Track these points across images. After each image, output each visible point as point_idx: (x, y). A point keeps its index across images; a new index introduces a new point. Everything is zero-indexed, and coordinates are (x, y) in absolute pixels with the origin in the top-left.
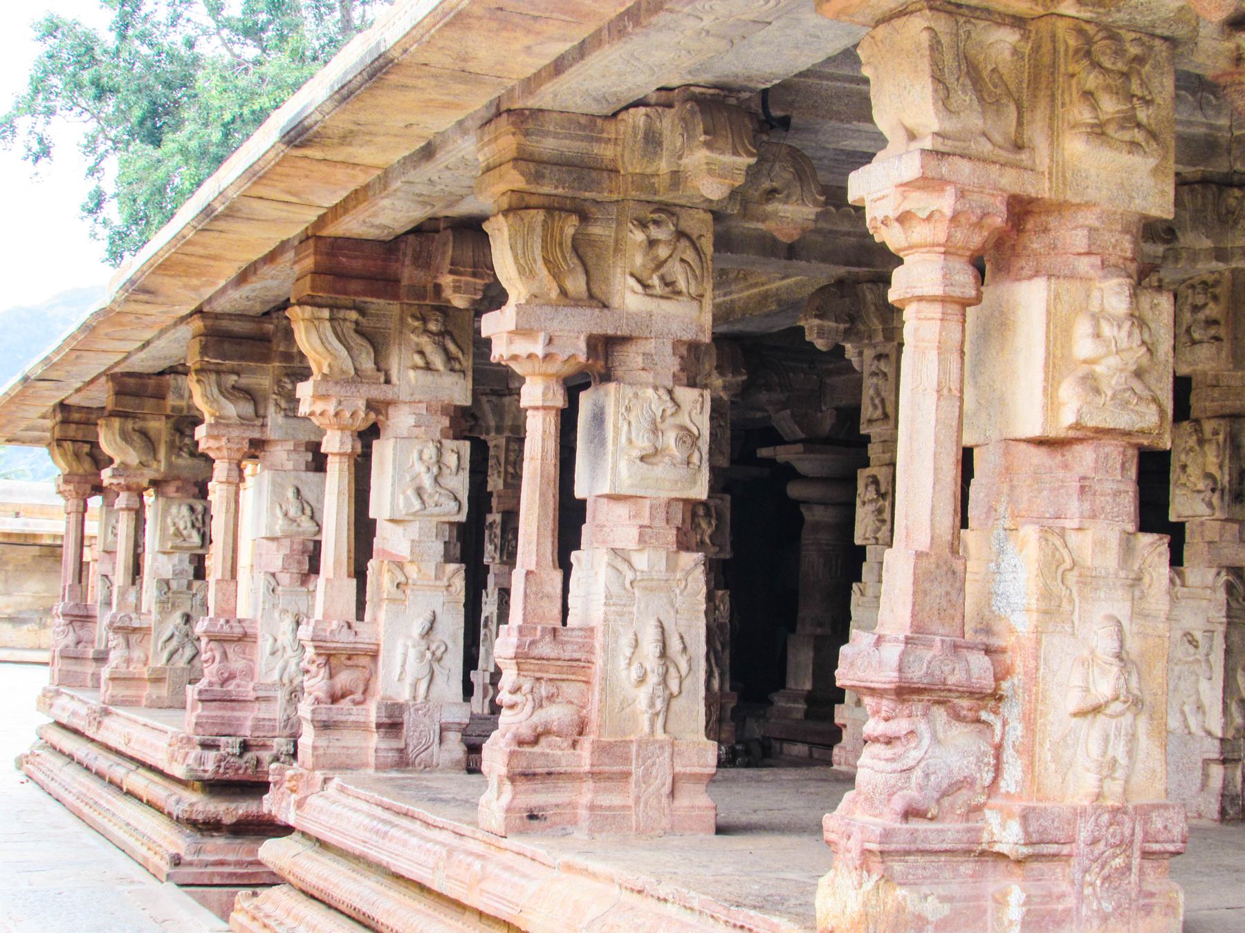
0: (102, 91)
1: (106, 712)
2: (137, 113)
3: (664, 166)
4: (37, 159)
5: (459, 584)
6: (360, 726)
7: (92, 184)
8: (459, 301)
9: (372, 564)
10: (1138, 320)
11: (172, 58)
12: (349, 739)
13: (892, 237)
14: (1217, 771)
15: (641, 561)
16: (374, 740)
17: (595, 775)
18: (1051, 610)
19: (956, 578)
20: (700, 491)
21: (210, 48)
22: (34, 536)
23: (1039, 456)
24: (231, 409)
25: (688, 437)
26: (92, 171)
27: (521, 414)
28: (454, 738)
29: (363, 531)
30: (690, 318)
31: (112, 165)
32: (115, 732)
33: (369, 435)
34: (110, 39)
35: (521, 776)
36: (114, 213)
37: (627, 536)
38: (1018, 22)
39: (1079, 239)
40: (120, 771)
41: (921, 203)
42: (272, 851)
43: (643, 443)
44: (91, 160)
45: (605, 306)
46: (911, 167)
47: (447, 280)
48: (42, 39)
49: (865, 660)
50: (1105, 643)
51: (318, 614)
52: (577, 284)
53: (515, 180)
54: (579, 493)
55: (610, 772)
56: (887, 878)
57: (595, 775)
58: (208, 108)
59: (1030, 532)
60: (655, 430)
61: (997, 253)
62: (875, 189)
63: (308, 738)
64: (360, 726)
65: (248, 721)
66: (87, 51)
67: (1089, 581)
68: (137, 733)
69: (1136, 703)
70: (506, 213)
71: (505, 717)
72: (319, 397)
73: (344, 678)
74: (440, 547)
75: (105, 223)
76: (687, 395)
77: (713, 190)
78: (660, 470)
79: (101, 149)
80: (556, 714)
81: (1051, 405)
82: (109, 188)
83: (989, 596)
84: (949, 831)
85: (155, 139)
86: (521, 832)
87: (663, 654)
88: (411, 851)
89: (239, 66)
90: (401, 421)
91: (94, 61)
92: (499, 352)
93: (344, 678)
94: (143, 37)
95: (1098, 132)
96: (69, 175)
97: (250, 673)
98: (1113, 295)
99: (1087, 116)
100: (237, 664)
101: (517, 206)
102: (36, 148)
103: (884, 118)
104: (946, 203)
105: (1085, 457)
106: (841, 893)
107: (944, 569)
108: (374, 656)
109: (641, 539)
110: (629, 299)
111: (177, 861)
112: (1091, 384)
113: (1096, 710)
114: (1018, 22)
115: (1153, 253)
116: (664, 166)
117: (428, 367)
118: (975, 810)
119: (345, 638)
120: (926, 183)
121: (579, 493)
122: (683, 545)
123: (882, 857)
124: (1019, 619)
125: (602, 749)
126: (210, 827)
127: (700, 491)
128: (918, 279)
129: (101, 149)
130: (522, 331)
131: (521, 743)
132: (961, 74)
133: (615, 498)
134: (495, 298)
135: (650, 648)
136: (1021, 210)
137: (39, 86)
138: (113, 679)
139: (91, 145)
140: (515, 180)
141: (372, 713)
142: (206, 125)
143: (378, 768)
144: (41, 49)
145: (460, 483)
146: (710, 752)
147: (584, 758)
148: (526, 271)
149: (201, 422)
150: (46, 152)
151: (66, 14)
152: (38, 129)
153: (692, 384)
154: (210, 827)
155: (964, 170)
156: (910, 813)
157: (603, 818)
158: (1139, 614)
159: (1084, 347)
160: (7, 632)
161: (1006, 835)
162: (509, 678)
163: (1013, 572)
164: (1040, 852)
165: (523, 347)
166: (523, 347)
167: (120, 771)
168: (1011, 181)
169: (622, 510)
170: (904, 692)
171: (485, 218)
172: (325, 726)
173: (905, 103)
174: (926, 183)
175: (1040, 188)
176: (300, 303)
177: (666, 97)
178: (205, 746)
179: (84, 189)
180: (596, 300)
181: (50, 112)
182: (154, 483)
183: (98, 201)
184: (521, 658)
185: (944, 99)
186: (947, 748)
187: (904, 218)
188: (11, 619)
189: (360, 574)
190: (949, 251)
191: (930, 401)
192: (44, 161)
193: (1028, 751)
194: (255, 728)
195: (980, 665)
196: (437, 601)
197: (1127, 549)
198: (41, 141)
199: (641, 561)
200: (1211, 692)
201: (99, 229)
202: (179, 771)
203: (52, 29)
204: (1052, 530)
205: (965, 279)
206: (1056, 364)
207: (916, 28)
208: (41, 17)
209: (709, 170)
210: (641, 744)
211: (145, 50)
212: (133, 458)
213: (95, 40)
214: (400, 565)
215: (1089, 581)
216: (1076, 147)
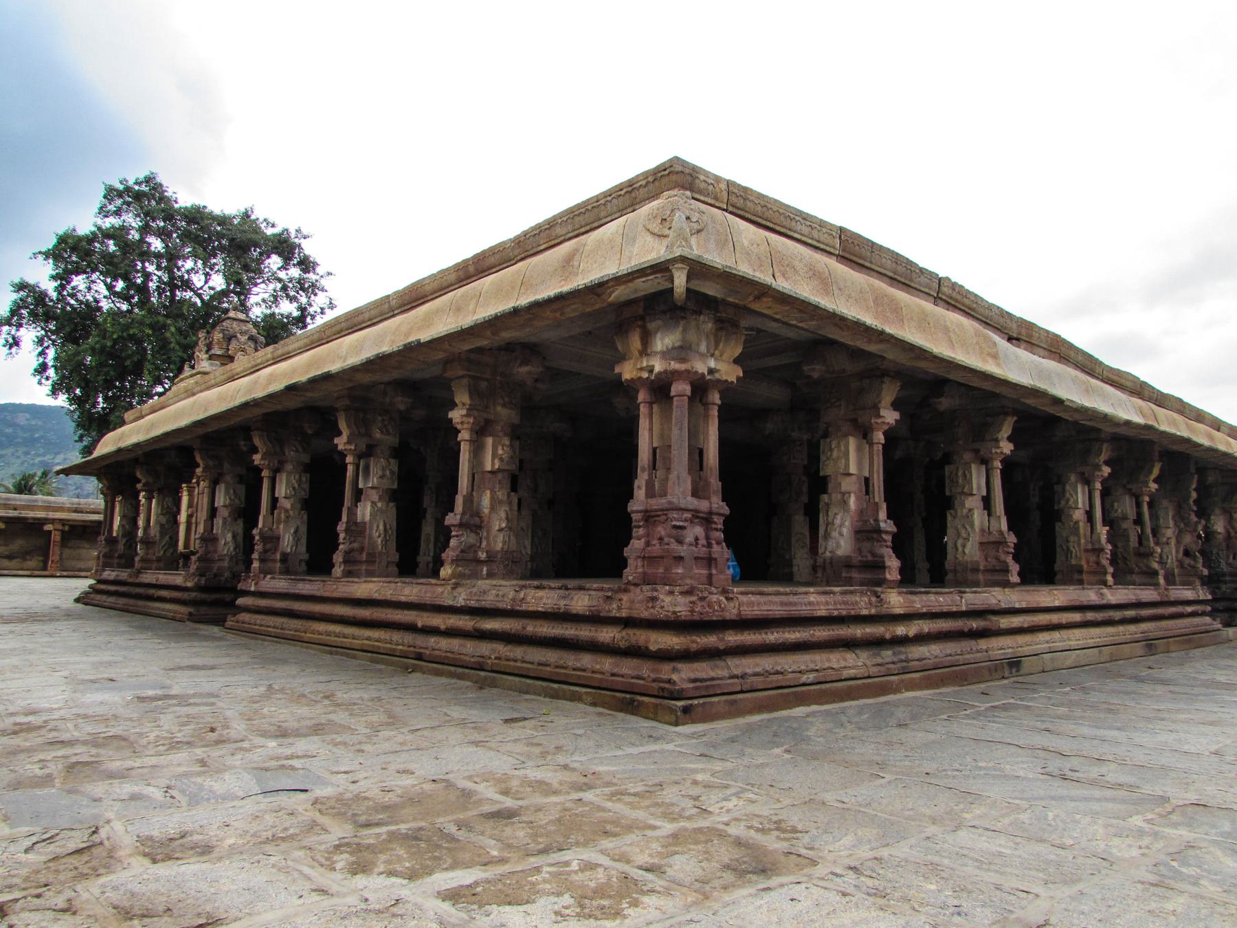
0: (48, 316)
1: (139, 572)
2: (68, 329)
3: (388, 400)
4: (11, 347)
5: (305, 517)
6: (274, 561)
7: (41, 360)
8: (310, 432)
9: (276, 512)
10: (511, 446)
11: (87, 304)
12: (270, 564)
13: (459, 427)
14: (529, 564)
15: (379, 505)
16: (278, 565)
17: (367, 561)
18: (492, 508)
19: (472, 502)
20: (395, 486)
21: (105, 305)
22: (26, 519)
23: (489, 475)
24: (211, 463)
25: (392, 472)
26: (40, 354)
27: (346, 465)
28: (303, 564)
29: (274, 501)
30: (392, 440)
31: (51, 353)
32: (148, 577)
33: (276, 471)
34: (54, 295)
35: (346, 562)
36: (51, 372)
37: (375, 498)
38: (487, 380)
39: (499, 428)
40: (151, 591)
41: (465, 419)
42: (241, 601)
43: (380, 473)
44: (40, 349)
45: (370, 436)
46: (464, 412)
47: (306, 425)
48: (17, 292)
49: (451, 519)
50: (503, 515)
51: (260, 525)
52: (363, 431)
53: (348, 402)
54: (361, 486)
55: (371, 559)
56: (457, 566)
57: (367, 561)
58: (105, 330)
59: (488, 492)
60: (383, 469)
61: (481, 431)
62: (456, 415)
63: (256, 564)
64: (274, 561)
65: (215, 566)
66: (41, 297)
67: (501, 502)
68: (161, 577)
69: (510, 529)
70: (345, 410)
71: (341, 547)
72: (262, 459)
73: (268, 546)
74: (299, 506)
75: (47, 378)
76: (392, 461)
77: (402, 407)
78: (385, 481)
79: (46, 344)
80: (355, 545)
81: (493, 464)
82: (51, 364)
83: (479, 505)
84: (471, 556)
85: (75, 341)
86: (347, 577)
87: (385, 529)
88: (305, 588)
89: (122, 312)
90: (289, 467)
91: (45, 305)
92: (340, 447)
93: (268, 546)
94: (73, 296)
95: (504, 406)
96: (28, 354)
97: (215, 551)
98: (507, 441)
99: (501, 401)
100: (211, 548)
101: (347, 409)
102: (11, 341)
103: (457, 401)
104: (471, 420)
105: (500, 476)
106: (446, 571)
107: (469, 499)
108: (278, 538)
109: (380, 499)
110: (378, 435)
111: (190, 614)
112: (501, 460)
113: (501, 530)
114: (487, 380)
115: (515, 434)
116: (388, 400)
117: (297, 451)
118: (476, 552)
119: (270, 533)
120: (467, 415)
121: (361, 486)
122: (390, 501)
123: (456, 561)
124: (486, 511)
125: (369, 554)
126: (202, 603)
127: (395, 486)
128: (464, 435)
129: (46, 344)
130: (349, 442)
131: (346, 552)
132: (474, 392)
133: (372, 488)
134: (340, 434)
135: (381, 527)
136: (488, 422)
137: (15, 312)
138: (142, 560)
139: (40, 341)
140: (348, 402)
141: (278, 557)
142: (104, 338)
143: (281, 573)
144: (15, 296)
145: (306, 486)
146: (396, 557)
147: (364, 557)
148: (349, 427)
149: (198, 466)
150: (16, 343)
151: (32, 281)
152: (13, 332)
153: (394, 458)
154: (202, 603)
155: (476, 413)
156: (462, 551)
157: (370, 574)
158: (511, 510)
159: (500, 452)
160: (6, 563)
161: (483, 556)
162: (342, 536)
163: (486, 501)
164: (490, 560)
165: (348, 447)
166: (348, 447)
167: (151, 591)
168: (485, 415)
169: (374, 491)
170: (461, 525)
171: (337, 410)
172: (262, 560)
173: (462, 397)
174: (467, 415)
175: (492, 417)
176: (257, 429)
177: (389, 383)
178: (201, 575)
179: (35, 363)
180: (368, 435)
181: (20, 326)
182: (160, 491)
183: (42, 369)
184: (347, 531)
185: (471, 398)
186: (470, 538)
187: (462, 423)
188: (10, 557)
189: (272, 514)
190: (471, 430)
191: (466, 464)
192: (14, 349)
193: (488, 538)
194: (219, 568)
195: (477, 519)
196: (299, 523)
197: (509, 496)
198: (14, 338)
199: (379, 505)
200: (528, 543)
201: (43, 381)
202: (189, 584)
203: (21, 286)
204: (493, 492)
205: (475, 436)
206: (494, 455)
207: (465, 381)
208: (17, 281)
209: (401, 403)
210: (380, 553)
211: (73, 302)
212: (151, 480)
213: (46, 295)
214: (286, 511)
215: (501, 502)
216: (499, 408)
